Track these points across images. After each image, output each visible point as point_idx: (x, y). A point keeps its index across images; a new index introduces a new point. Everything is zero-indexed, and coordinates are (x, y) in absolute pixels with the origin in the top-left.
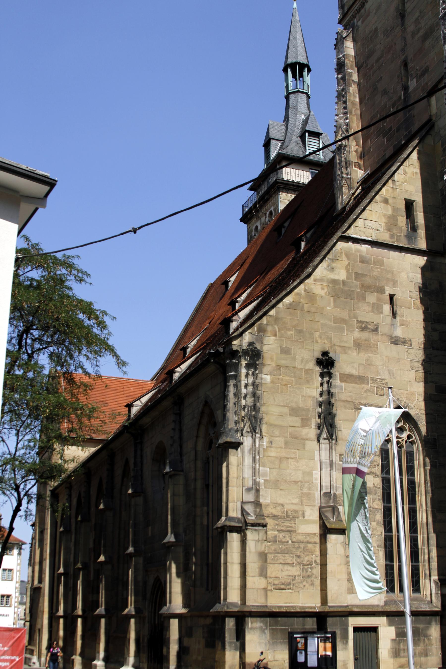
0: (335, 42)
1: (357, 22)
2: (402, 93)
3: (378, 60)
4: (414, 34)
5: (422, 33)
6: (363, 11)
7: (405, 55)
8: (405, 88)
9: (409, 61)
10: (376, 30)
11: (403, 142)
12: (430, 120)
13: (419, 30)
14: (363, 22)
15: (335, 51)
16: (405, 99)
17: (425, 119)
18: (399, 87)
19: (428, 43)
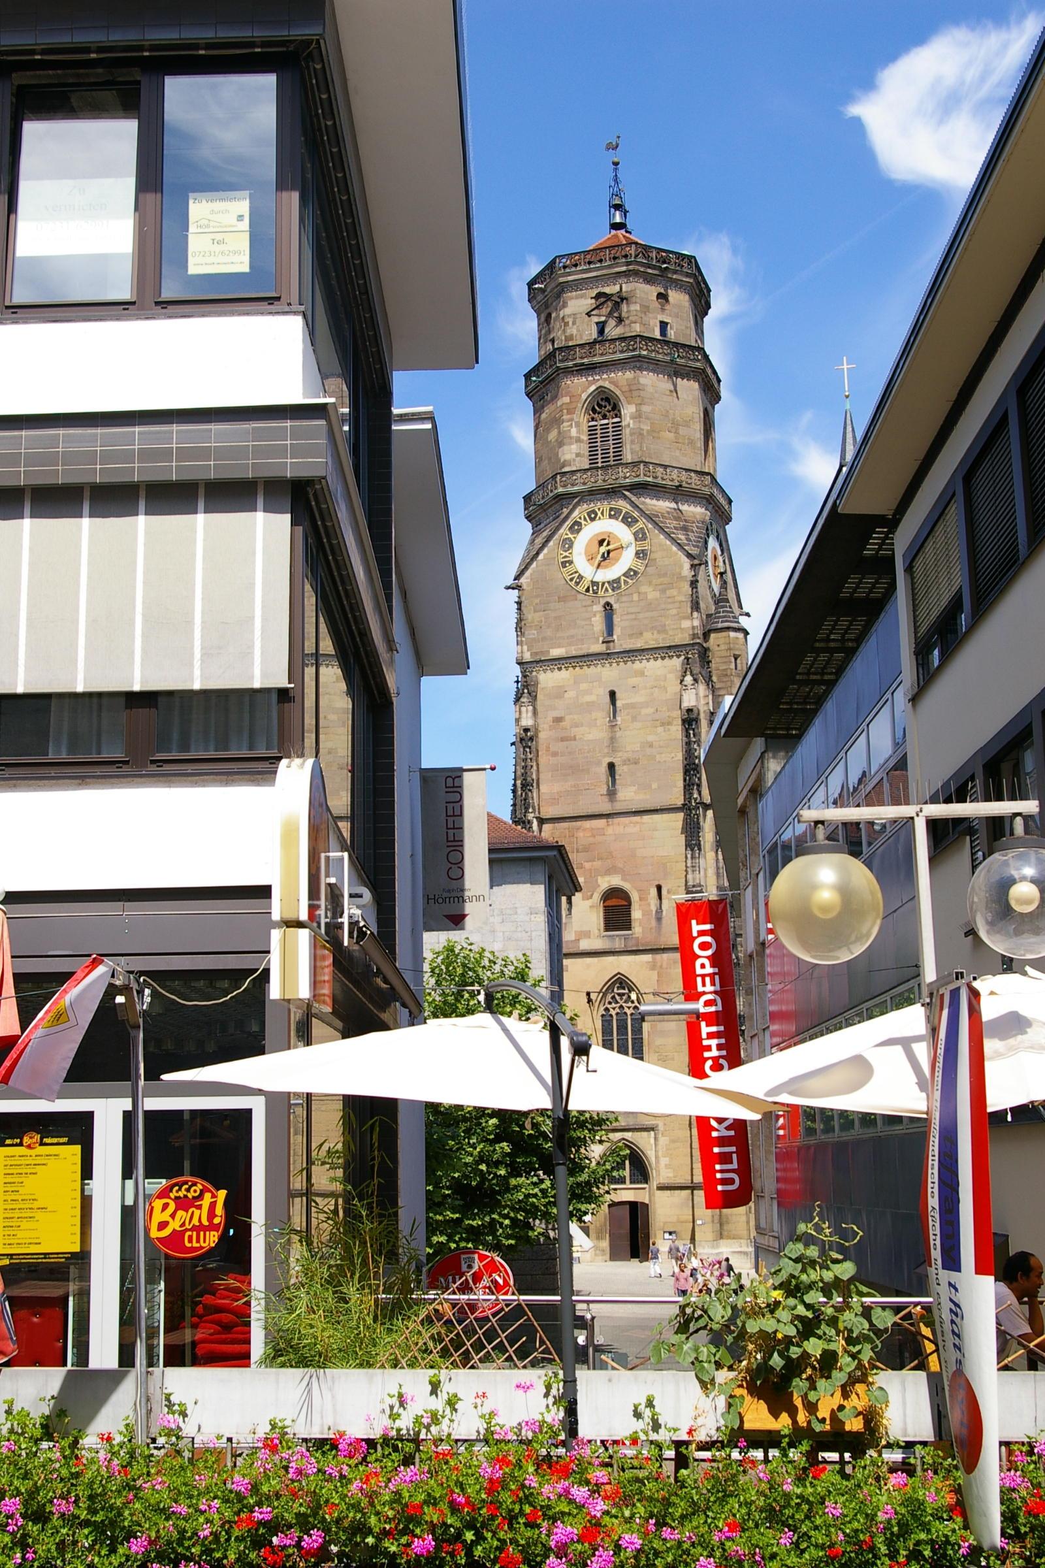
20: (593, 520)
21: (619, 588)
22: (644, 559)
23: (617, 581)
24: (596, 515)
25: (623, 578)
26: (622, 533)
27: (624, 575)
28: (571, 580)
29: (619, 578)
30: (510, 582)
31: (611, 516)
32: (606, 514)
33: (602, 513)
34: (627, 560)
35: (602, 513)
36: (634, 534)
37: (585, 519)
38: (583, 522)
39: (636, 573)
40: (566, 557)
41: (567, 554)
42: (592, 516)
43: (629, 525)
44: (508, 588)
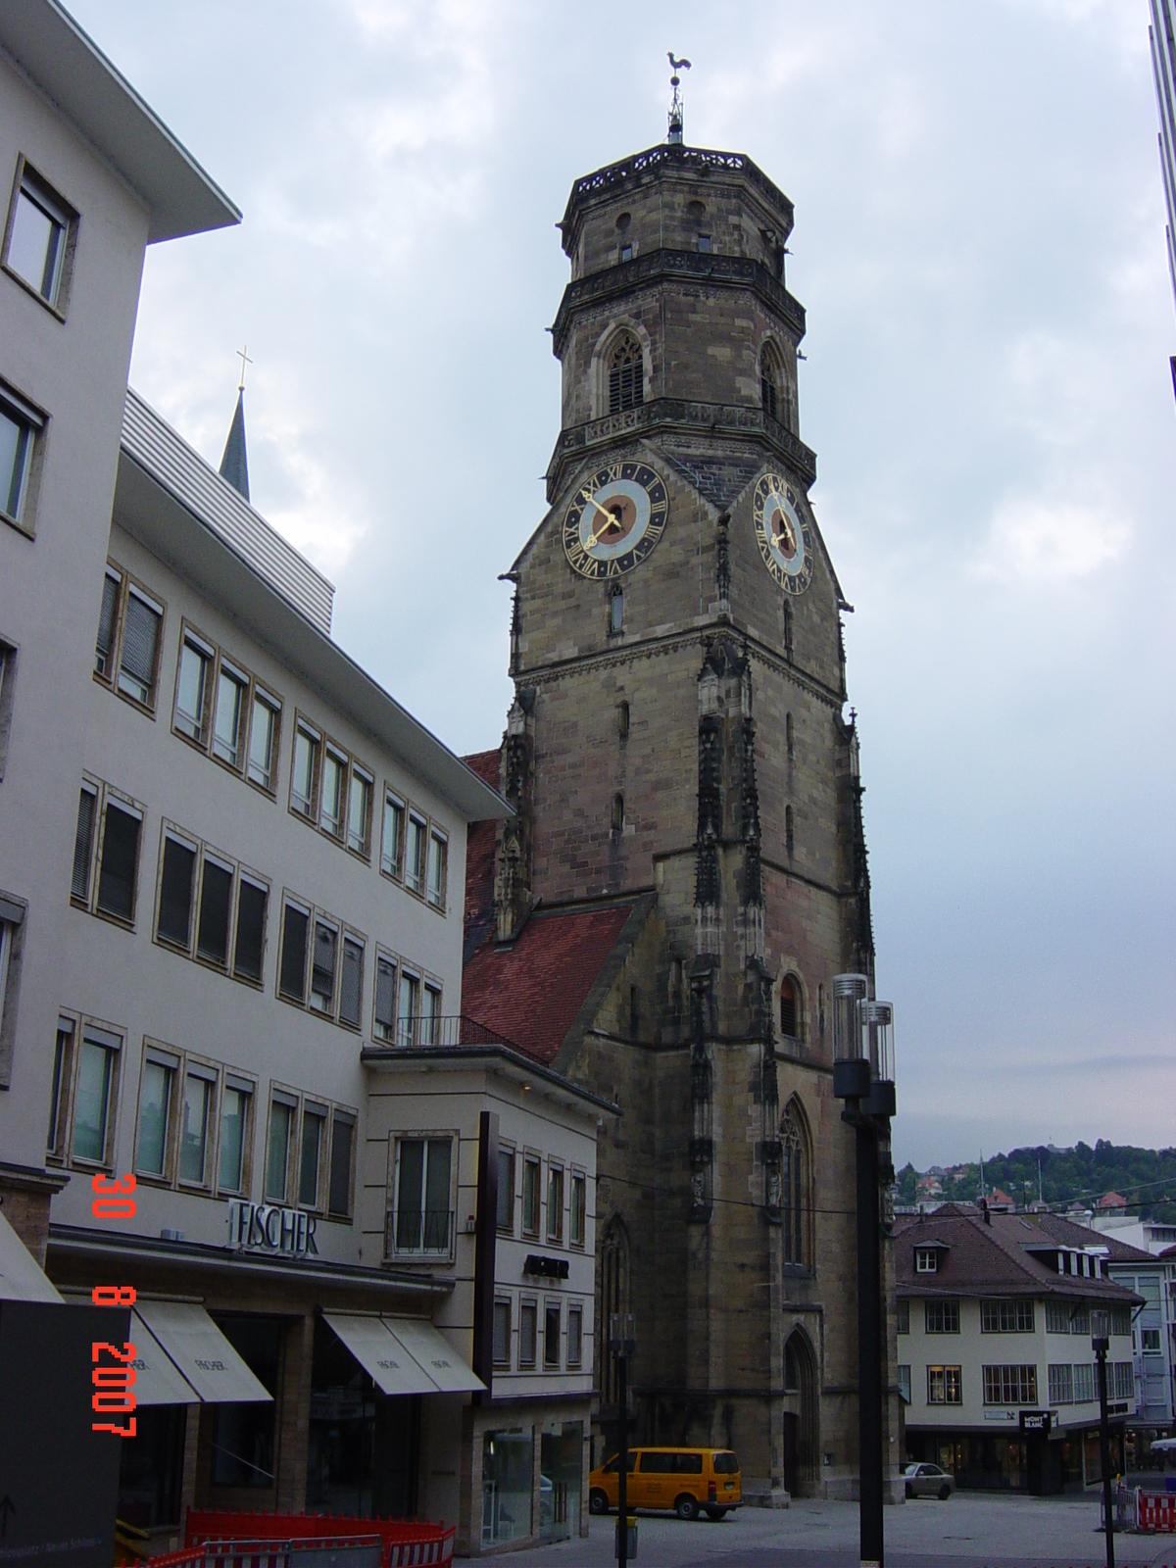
0: (509, 708)
1: (542, 693)
2: (611, 831)
3: (573, 766)
4: (638, 772)
5: (651, 777)
6: (553, 684)
7: (619, 788)
8: (617, 828)
9: (627, 797)
10: (575, 725)
11: (605, 891)
12: (652, 888)
13: (648, 771)
14: (553, 699)
15: (506, 720)
16: (614, 840)
17: (646, 882)
18: (606, 821)
19: (660, 795)
20: (603, 483)
21: (631, 563)
23: (629, 556)
24: (607, 475)
25: (635, 551)
26: (638, 496)
27: (636, 548)
28: (575, 562)
30: (505, 572)
32: (619, 475)
33: (615, 474)
34: (640, 527)
35: (615, 474)
36: (649, 493)
37: (595, 485)
41: (572, 530)
42: (603, 479)
43: (644, 484)
44: (501, 578)
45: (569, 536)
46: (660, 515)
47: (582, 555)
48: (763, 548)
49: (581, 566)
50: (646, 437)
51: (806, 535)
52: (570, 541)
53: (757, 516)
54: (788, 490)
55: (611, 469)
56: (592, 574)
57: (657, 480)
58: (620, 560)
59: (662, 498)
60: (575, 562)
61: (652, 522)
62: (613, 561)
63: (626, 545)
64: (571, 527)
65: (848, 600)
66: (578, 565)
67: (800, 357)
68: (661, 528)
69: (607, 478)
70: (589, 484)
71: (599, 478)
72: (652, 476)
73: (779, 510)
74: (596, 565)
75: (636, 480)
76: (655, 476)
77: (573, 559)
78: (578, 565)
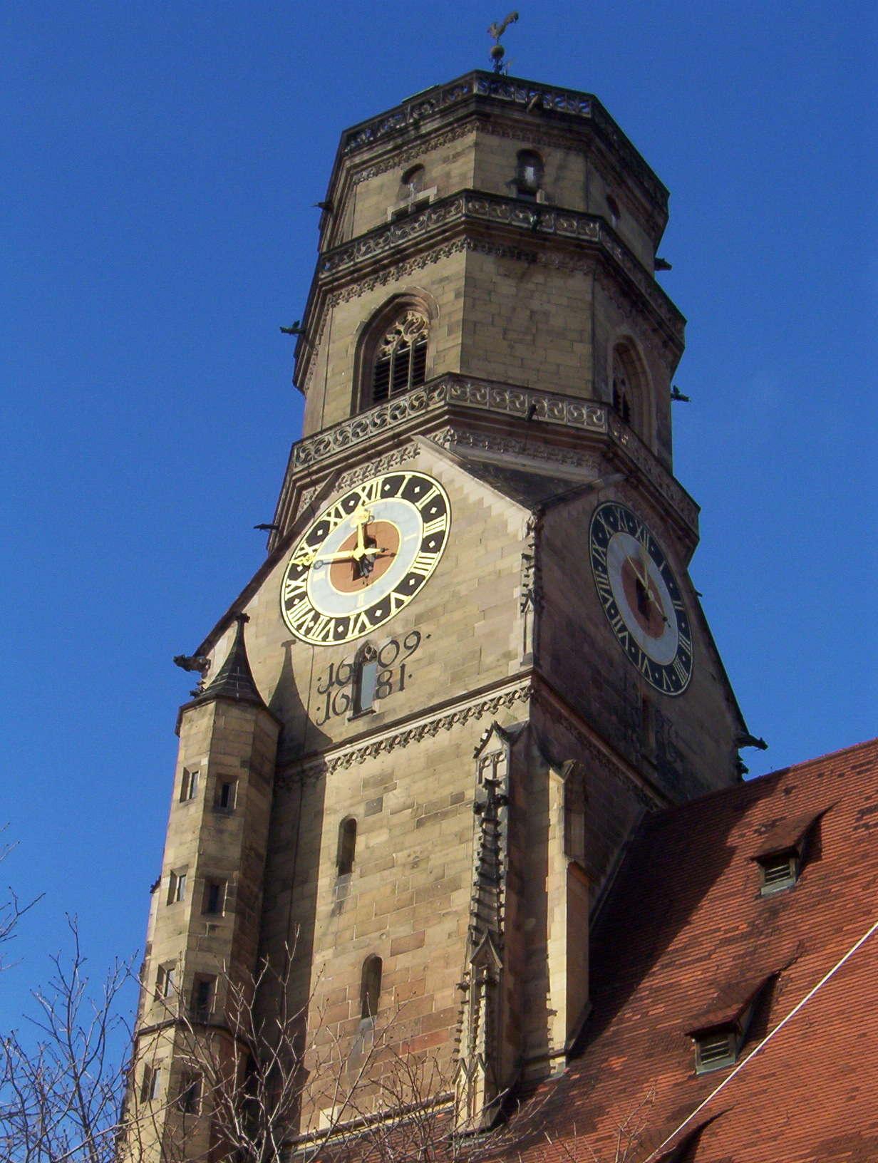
20: (349, 510)
21: (387, 612)
22: (436, 549)
23: (385, 605)
24: (356, 497)
25: (394, 596)
27: (396, 590)
28: (300, 627)
29: (389, 595)
31: (385, 495)
33: (369, 496)
35: (369, 496)
37: (338, 515)
38: (332, 519)
39: (420, 578)
40: (297, 588)
45: (292, 591)
46: (439, 537)
47: (313, 612)
48: (606, 600)
49: (308, 631)
50: (424, 433)
51: (681, 616)
52: (292, 599)
53: (596, 551)
54: (652, 543)
55: (364, 489)
56: (325, 638)
57: (435, 491)
58: (370, 613)
59: (442, 511)
60: (300, 627)
61: (425, 548)
62: (359, 615)
63: (385, 583)
64: (296, 579)
65: (754, 732)
66: (303, 631)
67: (679, 398)
68: (438, 556)
69: (356, 505)
70: (329, 515)
71: (345, 504)
72: (426, 486)
73: (626, 561)
74: (333, 623)
75: (404, 496)
76: (431, 485)
77: (295, 625)
78: (303, 631)
